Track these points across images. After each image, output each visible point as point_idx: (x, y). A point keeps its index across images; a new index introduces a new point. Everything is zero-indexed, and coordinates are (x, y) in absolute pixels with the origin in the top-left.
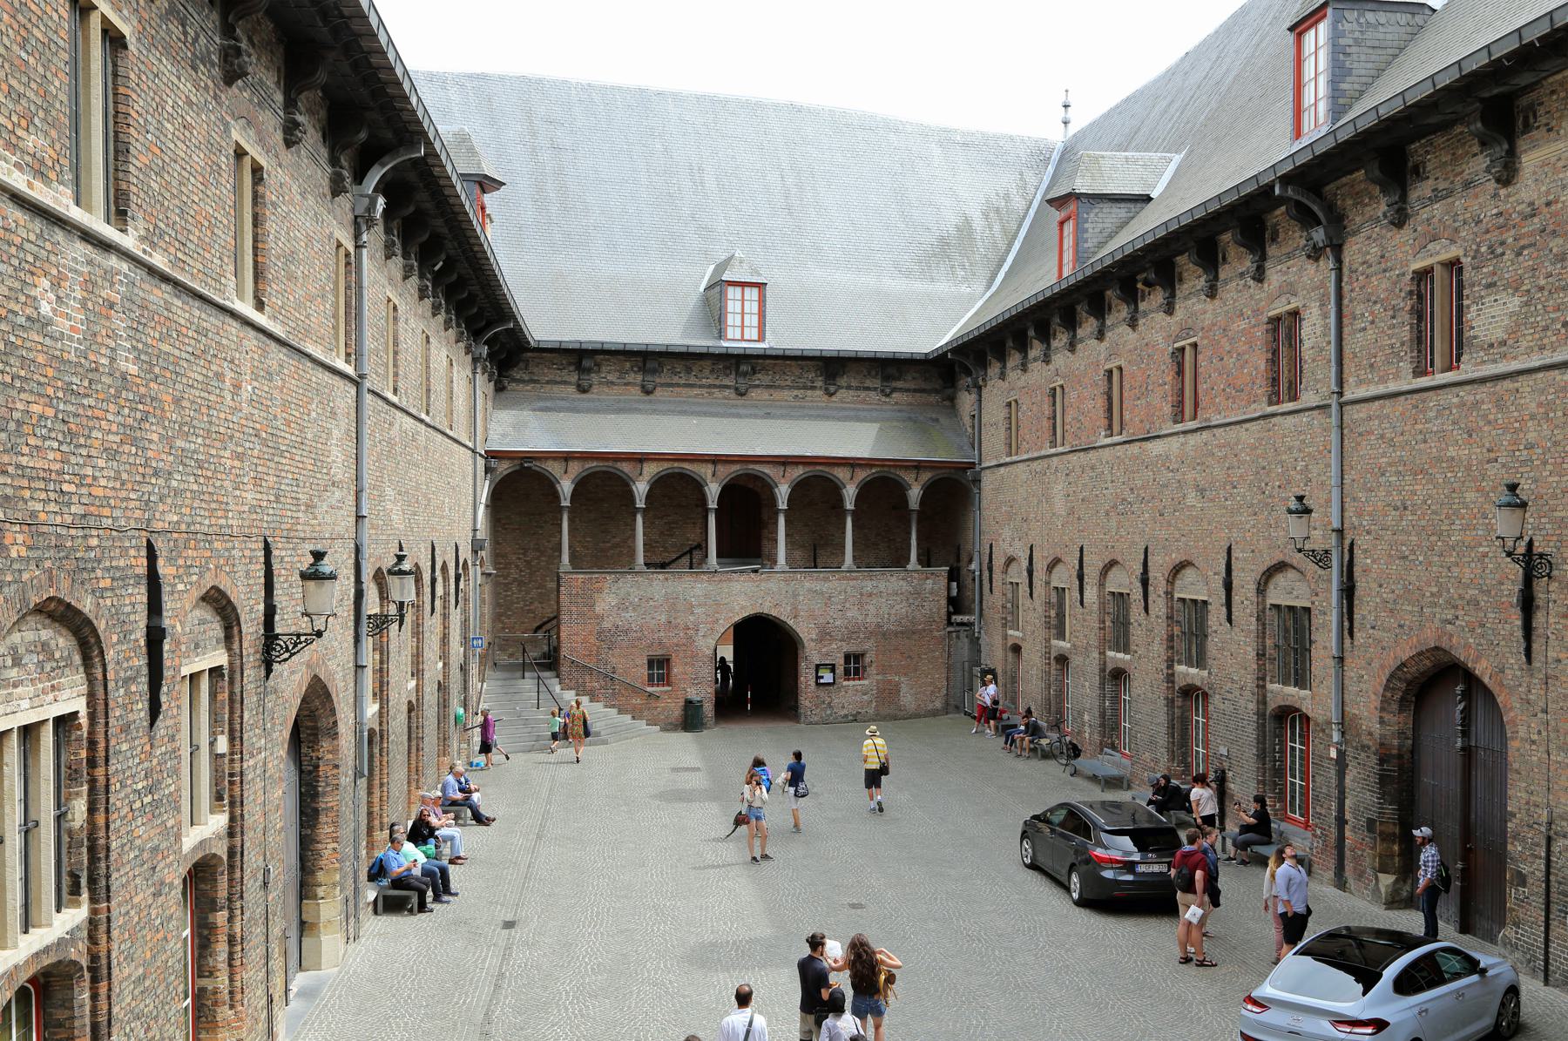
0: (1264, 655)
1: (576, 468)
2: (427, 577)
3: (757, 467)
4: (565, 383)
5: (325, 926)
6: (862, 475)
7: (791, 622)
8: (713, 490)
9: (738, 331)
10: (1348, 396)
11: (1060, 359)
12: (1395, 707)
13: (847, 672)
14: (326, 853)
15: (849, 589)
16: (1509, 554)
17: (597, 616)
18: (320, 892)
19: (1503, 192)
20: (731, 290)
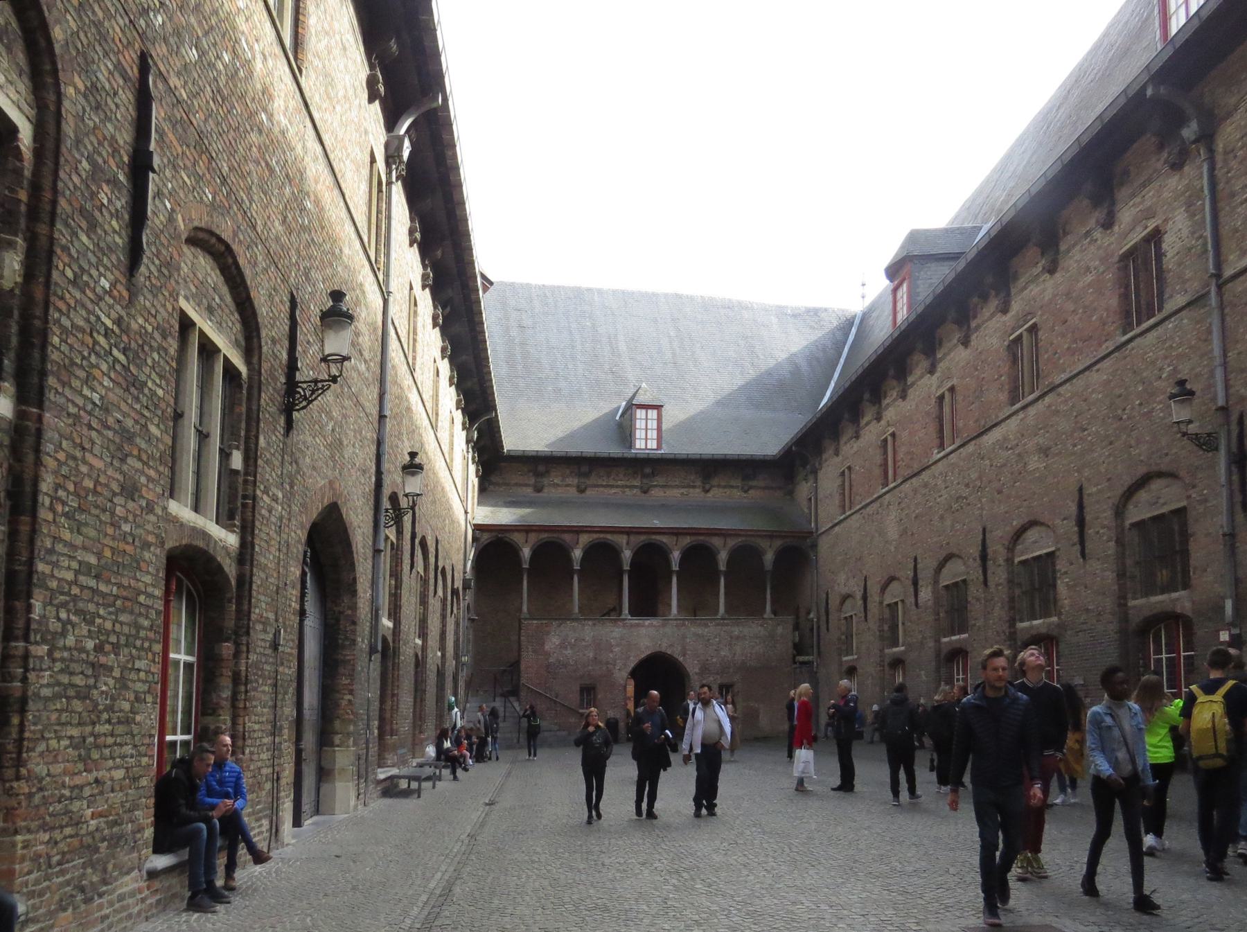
3: (658, 537)
5: (340, 774)
6: (732, 543)
10: (1228, 272)
11: (890, 414)
14: (344, 703)
18: (337, 739)
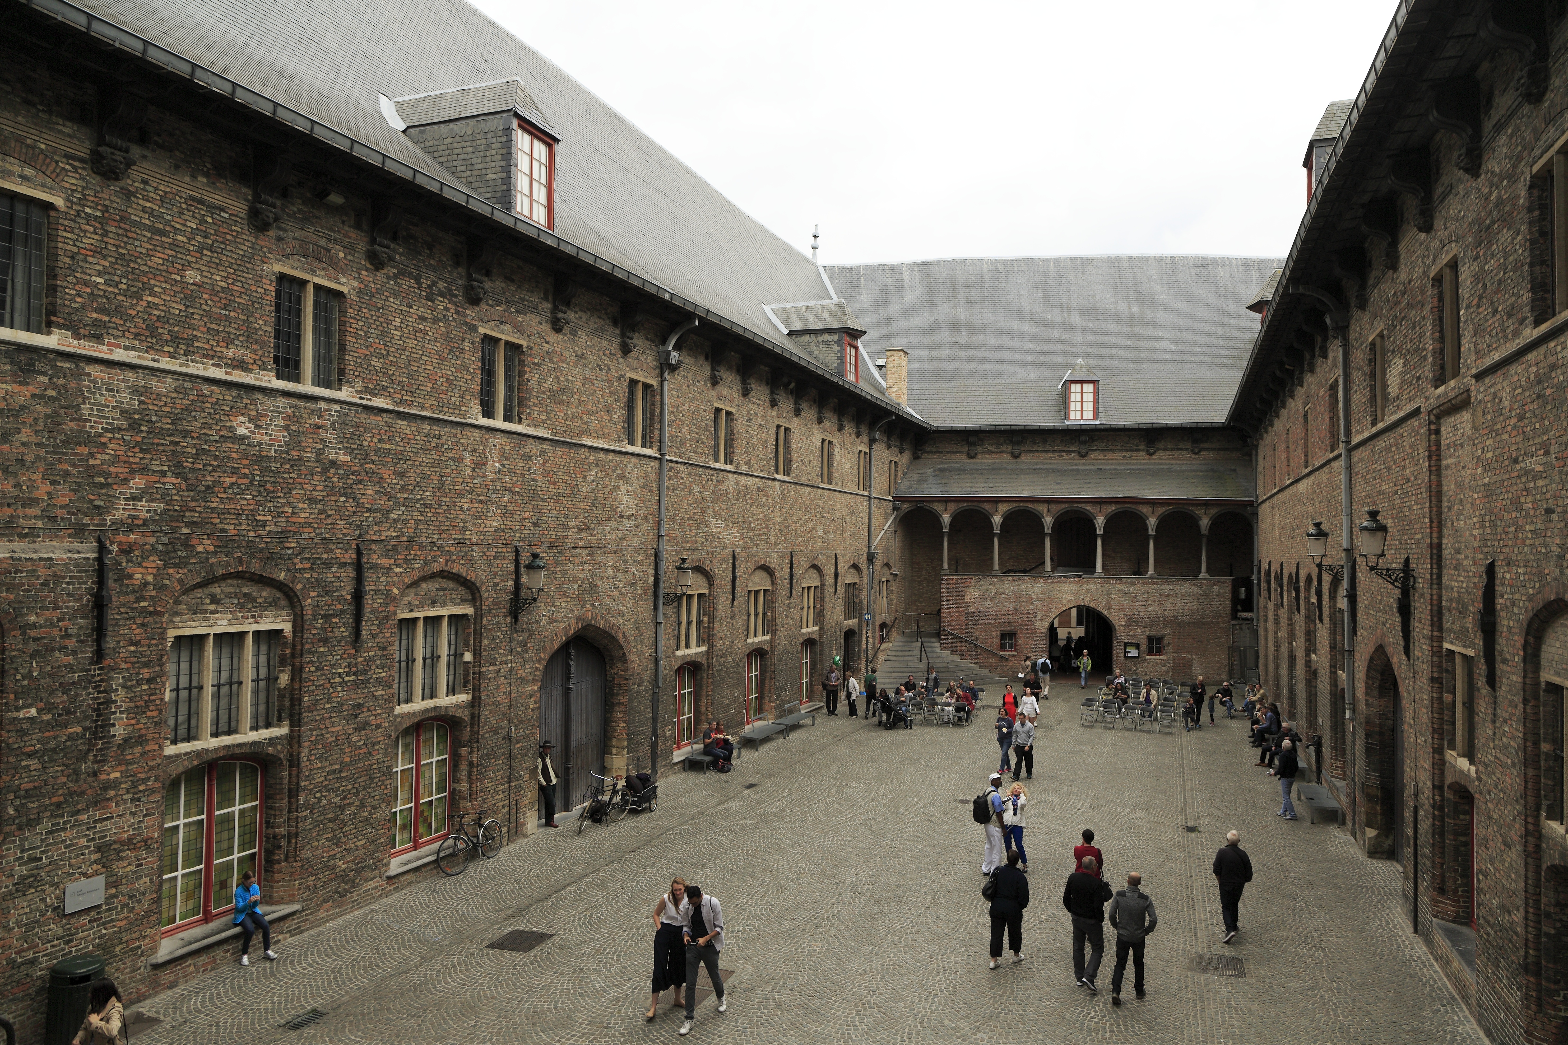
0: (1335, 648)
1: (952, 507)
2: (782, 572)
3: (1080, 505)
6: (1161, 510)
7: (1105, 612)
9: (1079, 413)
14: (619, 729)
15: (1151, 591)
17: (966, 604)
18: (614, 751)
20: (1073, 387)
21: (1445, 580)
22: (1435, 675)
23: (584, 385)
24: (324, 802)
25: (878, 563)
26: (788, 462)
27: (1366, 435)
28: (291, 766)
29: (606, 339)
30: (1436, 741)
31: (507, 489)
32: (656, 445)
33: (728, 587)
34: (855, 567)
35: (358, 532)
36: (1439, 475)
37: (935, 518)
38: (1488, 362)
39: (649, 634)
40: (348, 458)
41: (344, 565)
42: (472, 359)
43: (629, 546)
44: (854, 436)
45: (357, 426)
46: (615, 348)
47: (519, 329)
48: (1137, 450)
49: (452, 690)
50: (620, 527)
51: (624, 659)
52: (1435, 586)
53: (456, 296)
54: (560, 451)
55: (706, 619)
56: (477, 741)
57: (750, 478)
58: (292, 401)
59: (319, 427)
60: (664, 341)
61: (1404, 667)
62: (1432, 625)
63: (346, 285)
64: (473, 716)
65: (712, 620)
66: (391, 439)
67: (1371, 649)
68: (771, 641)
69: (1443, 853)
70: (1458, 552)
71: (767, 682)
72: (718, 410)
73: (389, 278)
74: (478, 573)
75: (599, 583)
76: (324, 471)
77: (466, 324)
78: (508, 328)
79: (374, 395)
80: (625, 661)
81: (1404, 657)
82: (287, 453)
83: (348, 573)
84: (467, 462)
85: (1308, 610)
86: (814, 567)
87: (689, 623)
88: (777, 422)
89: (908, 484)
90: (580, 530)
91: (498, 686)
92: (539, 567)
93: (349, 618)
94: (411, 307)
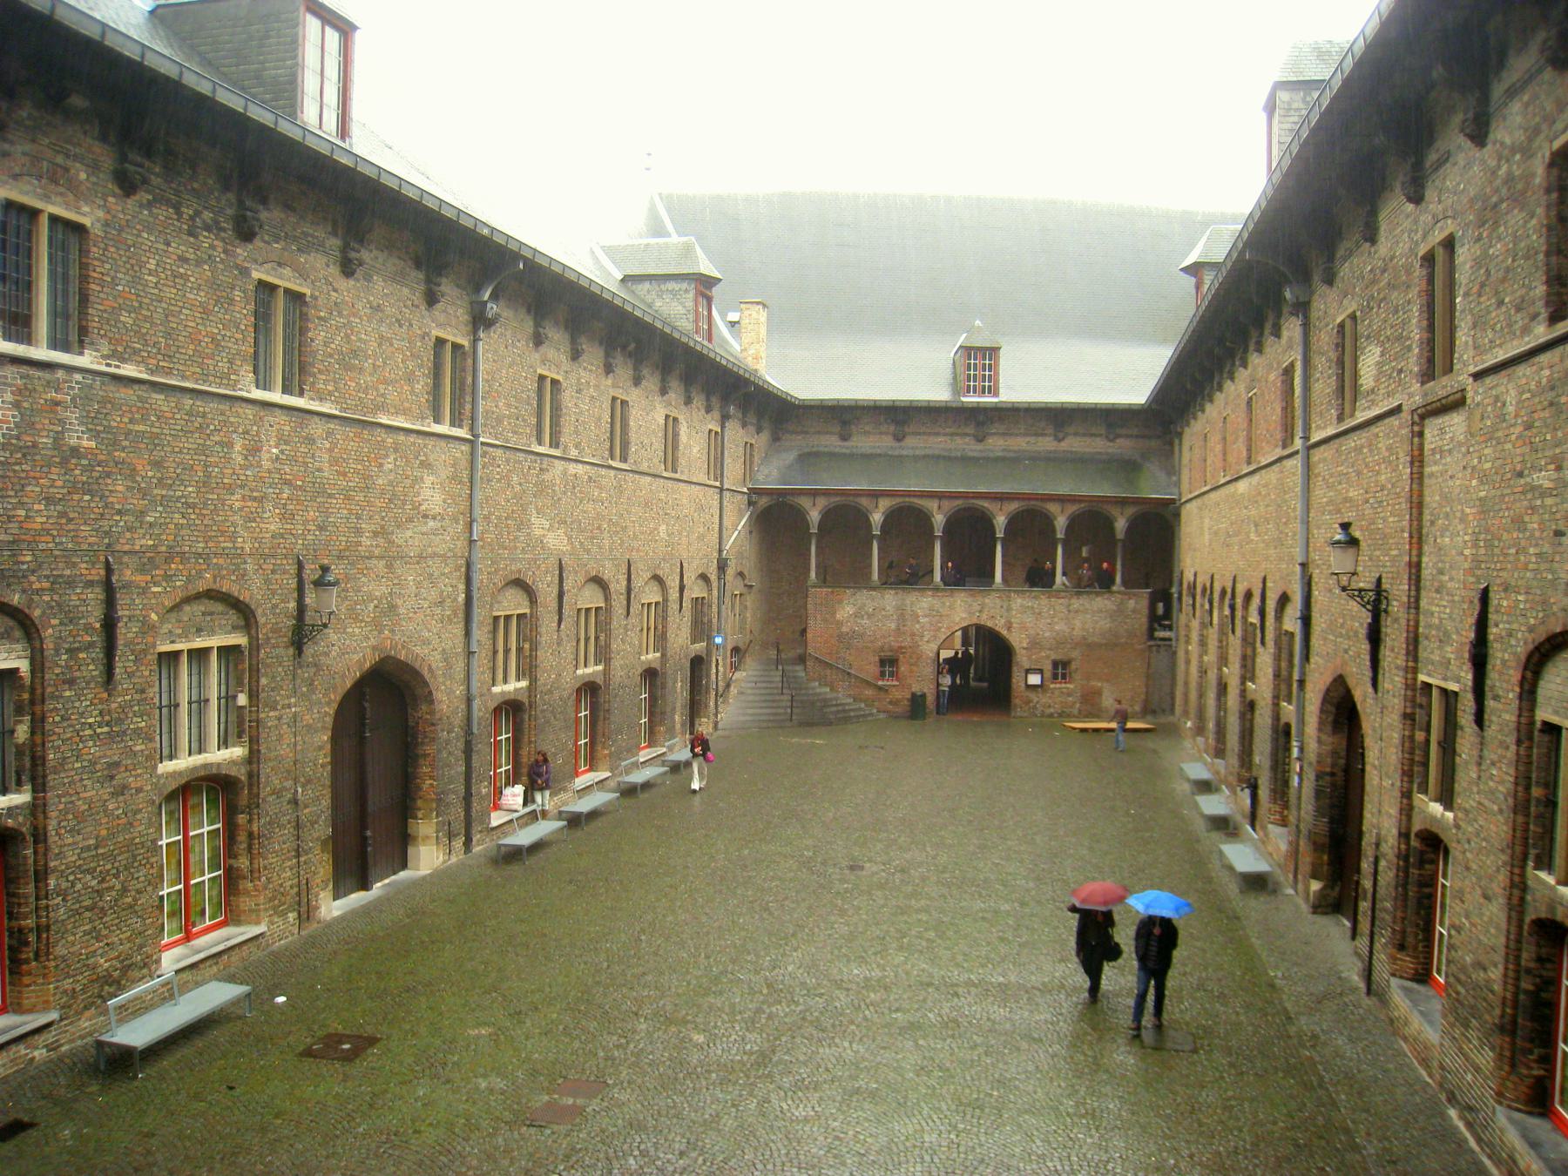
1: (822, 502)
2: (617, 586)
4: (831, 433)
7: (1004, 632)
8: (939, 520)
12: (1329, 728)
13: (1055, 676)
14: (425, 787)
16: (1344, 589)
18: (420, 814)
19: (1373, 250)
21: (1423, 603)
22: (1408, 711)
23: (380, 345)
24: (79, 886)
25: (730, 572)
26: (625, 445)
27: (1331, 431)
28: (36, 842)
29: (407, 286)
30: (1405, 785)
31: (288, 483)
32: (467, 422)
33: (555, 605)
34: (704, 577)
35: (106, 541)
36: (1421, 484)
37: (800, 516)
38: (1490, 361)
39: (460, 666)
40: (93, 444)
41: (90, 584)
42: (243, 312)
43: (435, 555)
44: (703, 411)
45: (104, 402)
46: (418, 298)
47: (303, 274)
48: (1045, 435)
49: (224, 743)
50: (424, 529)
51: (429, 698)
52: (1413, 611)
53: (224, 230)
54: (350, 431)
55: (527, 646)
56: (258, 806)
57: (580, 466)
58: (24, 369)
59: (57, 404)
60: (478, 289)
61: (1369, 701)
62: (1407, 654)
63: (87, 216)
64: (250, 775)
65: (534, 648)
66: (144, 419)
67: (1328, 679)
68: (606, 672)
69: (1405, 906)
70: (1441, 572)
71: (600, 723)
72: (542, 378)
73: (141, 206)
74: (253, 591)
75: (400, 602)
76: (64, 462)
77: (237, 266)
78: (287, 271)
79: (123, 360)
80: (432, 702)
81: (1370, 690)
82: (18, 438)
83: (95, 595)
84: (238, 448)
85: (1245, 631)
86: (657, 578)
87: (507, 651)
88: (612, 392)
89: (766, 472)
90: (375, 534)
91: (281, 736)
92: (330, 584)
93: (98, 653)
94: (168, 244)
